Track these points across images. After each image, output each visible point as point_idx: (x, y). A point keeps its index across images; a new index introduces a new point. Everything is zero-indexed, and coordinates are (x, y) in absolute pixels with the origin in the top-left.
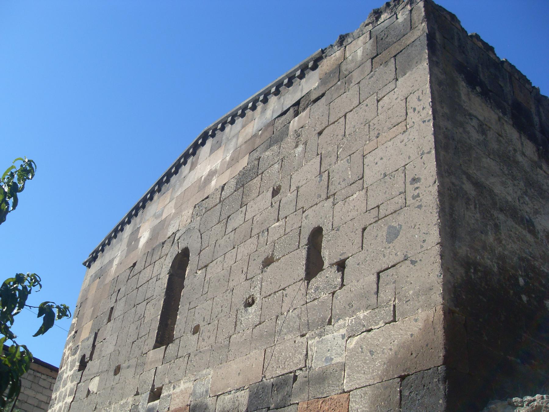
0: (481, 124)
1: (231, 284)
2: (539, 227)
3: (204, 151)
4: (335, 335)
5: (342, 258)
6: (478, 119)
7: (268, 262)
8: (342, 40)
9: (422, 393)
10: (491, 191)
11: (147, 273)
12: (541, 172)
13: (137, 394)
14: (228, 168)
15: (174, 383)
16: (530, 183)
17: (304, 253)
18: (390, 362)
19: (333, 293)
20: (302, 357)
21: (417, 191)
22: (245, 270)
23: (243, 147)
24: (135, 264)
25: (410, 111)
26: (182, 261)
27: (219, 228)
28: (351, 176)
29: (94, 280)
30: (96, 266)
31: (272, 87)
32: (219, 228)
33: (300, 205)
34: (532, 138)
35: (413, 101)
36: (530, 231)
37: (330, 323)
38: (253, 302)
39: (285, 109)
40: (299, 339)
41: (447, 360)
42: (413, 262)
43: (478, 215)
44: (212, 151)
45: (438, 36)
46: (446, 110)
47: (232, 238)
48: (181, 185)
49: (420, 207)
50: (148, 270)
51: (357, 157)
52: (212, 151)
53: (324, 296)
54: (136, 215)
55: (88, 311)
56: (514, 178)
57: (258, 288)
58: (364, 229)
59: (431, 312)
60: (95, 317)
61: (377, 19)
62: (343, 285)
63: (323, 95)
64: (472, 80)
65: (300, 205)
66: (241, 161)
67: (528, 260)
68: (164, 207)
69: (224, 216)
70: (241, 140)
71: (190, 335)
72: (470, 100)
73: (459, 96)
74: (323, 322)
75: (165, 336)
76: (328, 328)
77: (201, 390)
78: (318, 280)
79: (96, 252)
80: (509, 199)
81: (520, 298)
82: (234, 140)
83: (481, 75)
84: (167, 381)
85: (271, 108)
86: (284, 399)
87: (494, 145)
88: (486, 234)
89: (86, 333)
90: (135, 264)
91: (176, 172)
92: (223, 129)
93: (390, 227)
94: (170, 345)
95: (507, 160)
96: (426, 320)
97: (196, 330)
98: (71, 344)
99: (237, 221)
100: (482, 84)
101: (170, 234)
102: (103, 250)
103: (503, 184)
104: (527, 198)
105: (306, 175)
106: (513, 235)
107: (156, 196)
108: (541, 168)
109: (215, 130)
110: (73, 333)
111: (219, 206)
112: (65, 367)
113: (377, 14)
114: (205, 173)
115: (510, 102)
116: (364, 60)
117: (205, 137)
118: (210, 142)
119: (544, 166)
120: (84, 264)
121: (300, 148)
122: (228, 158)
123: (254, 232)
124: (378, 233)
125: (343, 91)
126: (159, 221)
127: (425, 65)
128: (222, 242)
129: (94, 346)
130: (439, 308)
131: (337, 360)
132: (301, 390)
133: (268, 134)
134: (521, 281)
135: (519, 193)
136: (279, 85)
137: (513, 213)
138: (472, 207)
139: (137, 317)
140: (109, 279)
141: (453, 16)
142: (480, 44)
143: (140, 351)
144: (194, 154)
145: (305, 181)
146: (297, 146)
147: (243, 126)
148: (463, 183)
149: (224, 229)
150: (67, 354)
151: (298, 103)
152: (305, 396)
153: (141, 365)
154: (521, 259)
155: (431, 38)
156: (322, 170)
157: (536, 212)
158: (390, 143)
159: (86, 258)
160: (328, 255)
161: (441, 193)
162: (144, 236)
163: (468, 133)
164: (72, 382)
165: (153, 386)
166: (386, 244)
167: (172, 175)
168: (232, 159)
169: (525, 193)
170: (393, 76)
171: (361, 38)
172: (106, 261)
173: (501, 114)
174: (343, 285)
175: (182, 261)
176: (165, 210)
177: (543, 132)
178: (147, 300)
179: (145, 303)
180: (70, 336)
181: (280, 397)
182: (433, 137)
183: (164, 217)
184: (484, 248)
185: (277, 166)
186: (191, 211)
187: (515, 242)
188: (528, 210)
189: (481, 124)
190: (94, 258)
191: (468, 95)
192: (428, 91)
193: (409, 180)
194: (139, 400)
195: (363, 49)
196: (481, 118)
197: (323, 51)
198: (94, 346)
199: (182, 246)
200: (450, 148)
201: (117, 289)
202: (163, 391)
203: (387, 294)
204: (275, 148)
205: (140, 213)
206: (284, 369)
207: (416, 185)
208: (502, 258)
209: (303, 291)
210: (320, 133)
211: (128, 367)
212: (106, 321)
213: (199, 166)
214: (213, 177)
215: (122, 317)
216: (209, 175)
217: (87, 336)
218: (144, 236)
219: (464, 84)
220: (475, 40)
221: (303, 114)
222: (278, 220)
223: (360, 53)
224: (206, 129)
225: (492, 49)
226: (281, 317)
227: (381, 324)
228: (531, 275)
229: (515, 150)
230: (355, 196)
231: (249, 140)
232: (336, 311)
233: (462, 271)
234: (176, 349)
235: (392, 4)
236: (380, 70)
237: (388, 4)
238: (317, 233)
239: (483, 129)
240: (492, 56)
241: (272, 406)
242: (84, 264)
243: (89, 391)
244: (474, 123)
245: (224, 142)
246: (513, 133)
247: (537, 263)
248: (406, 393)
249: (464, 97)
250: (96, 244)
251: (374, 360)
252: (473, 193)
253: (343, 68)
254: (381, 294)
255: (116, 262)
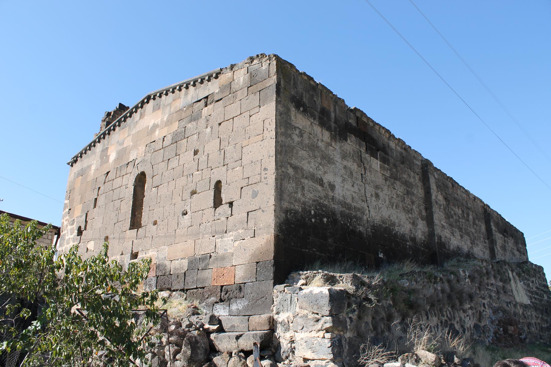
0: (301, 131)
1: (174, 201)
2: (325, 181)
3: (149, 107)
4: (229, 238)
5: (232, 200)
6: (299, 129)
7: (193, 193)
8: (232, 67)
9: (265, 270)
10: (302, 169)
11: (118, 182)
12: (331, 148)
13: (122, 254)
14: (165, 126)
15: (146, 250)
16: (323, 157)
17: (213, 193)
18: (253, 255)
19: (228, 218)
20: (213, 247)
21: (266, 176)
22: (181, 195)
23: (174, 114)
24: (108, 173)
25: (265, 129)
26: (141, 179)
27: (163, 165)
28: (236, 156)
29: (78, 177)
30: (78, 166)
31: (191, 81)
32: (163, 165)
33: (209, 166)
34: (329, 129)
35: (267, 125)
36: (320, 185)
37: (226, 232)
38: (187, 213)
39: (199, 99)
40: (211, 238)
41: (275, 258)
42: (263, 211)
43: (294, 185)
44: (154, 110)
45: (282, 82)
46: (283, 130)
47: (172, 173)
48: (135, 126)
49: (267, 184)
50: (119, 180)
51: (238, 147)
52: (154, 110)
53: (223, 219)
54: (104, 138)
55: (77, 197)
56: (315, 157)
57: (189, 207)
58: (242, 188)
59: (269, 236)
60: (82, 201)
61: (252, 62)
62: (232, 215)
63: (221, 99)
64: (299, 104)
65: (209, 166)
66: (173, 124)
67: (317, 200)
68: (125, 139)
69: (166, 158)
70: (172, 109)
71: (152, 225)
72: (296, 118)
73: (290, 118)
74: (223, 232)
75: (136, 223)
76: (225, 234)
77: (161, 256)
78: (220, 209)
79: (77, 157)
80: (311, 170)
81: (311, 221)
82: (168, 108)
83: (304, 99)
84: (140, 249)
85: (191, 94)
86: (206, 266)
87: (306, 141)
88: (297, 193)
89: (78, 212)
90: (108, 173)
91: (130, 116)
92: (160, 96)
93: (254, 191)
94: (140, 229)
95: (313, 148)
96: (267, 239)
97: (155, 223)
98: (67, 217)
99: (174, 163)
100: (304, 105)
101: (131, 159)
102: (81, 157)
103: (309, 163)
104: (321, 167)
105: (212, 147)
106: (311, 189)
107: (117, 128)
108: (331, 146)
109: (155, 96)
110: (67, 210)
111: (162, 150)
112: (66, 232)
113: (252, 59)
114: (151, 124)
115: (319, 110)
116: (244, 86)
117: (149, 98)
118: (151, 101)
119: (333, 144)
120: (68, 164)
121: (209, 129)
122: (165, 119)
123: (185, 174)
124: (248, 192)
125: (232, 102)
126: (121, 147)
127: (274, 104)
128: (166, 174)
129: (86, 222)
130: (273, 235)
131: (230, 251)
132: (214, 263)
133: (189, 112)
134: (313, 212)
135: (317, 165)
136: (195, 82)
137: (312, 177)
138: (291, 181)
139: (115, 208)
140: (90, 179)
141: (292, 65)
142: (306, 78)
143: (121, 230)
144: (142, 107)
145: (212, 152)
146: (207, 127)
147: (174, 100)
148: (288, 170)
149: (166, 166)
150: (65, 223)
151: (207, 97)
152: (215, 265)
153: (122, 239)
154: (314, 201)
155: (278, 85)
156: (221, 148)
157: (325, 173)
158: (255, 144)
159: (70, 160)
160: (225, 197)
161: (276, 179)
162: (113, 156)
163: (293, 139)
164: (73, 242)
165: (132, 251)
166: (251, 199)
167: (127, 117)
168: (168, 121)
169: (320, 164)
170: (258, 104)
171: (243, 70)
172: (85, 165)
173: (312, 121)
174: (232, 215)
175: (141, 179)
176: (126, 141)
177: (335, 122)
178: (121, 199)
179: (120, 200)
180: (65, 211)
181: (204, 265)
182: (274, 149)
183: (125, 146)
184: (296, 201)
185: (196, 136)
186: (144, 149)
187: (311, 193)
188: (320, 173)
189: (301, 131)
190: (75, 161)
191: (295, 115)
192: (274, 121)
193: (263, 168)
194: (124, 258)
195: (244, 78)
196: (301, 127)
197: (221, 70)
198: (86, 222)
199: (141, 170)
200: (283, 152)
201: (97, 187)
202: (139, 254)
203: (251, 224)
204: (194, 123)
205: (107, 137)
206: (205, 251)
207: (266, 172)
208: (304, 203)
209: (213, 214)
210: (220, 124)
211: (114, 238)
212: (92, 206)
213: (146, 117)
214: (156, 129)
215: (104, 206)
216: (153, 126)
217: (79, 214)
218: (113, 156)
219: (294, 109)
220: (303, 76)
221: (210, 107)
222: (198, 171)
223: (242, 79)
224: (149, 93)
225: (312, 79)
226: (202, 225)
227: (249, 237)
228: (318, 207)
229: (318, 140)
230: (237, 168)
231: (178, 111)
232: (229, 228)
233: (283, 215)
234: (144, 232)
235: (260, 56)
236: (251, 96)
237: (258, 56)
238: (218, 184)
239: (301, 135)
240: (312, 83)
241: (200, 269)
242: (68, 164)
243: (87, 249)
244: (297, 132)
245: (161, 107)
246: (317, 129)
247: (322, 201)
248: (259, 269)
249: (293, 118)
250: (76, 152)
251: (246, 253)
252: (293, 173)
253: (233, 86)
254: (249, 223)
255: (93, 168)
